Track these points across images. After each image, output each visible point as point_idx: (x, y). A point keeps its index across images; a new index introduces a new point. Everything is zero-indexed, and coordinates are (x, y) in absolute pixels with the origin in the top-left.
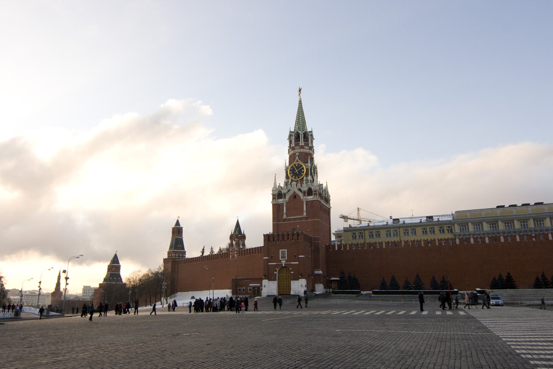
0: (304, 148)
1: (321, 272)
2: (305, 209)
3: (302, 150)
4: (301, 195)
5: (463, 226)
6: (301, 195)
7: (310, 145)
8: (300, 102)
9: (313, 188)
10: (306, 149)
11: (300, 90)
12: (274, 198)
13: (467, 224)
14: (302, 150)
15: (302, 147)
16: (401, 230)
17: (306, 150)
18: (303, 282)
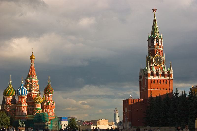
0: (151, 48)
3: (150, 49)
12: (140, 79)
14: (150, 49)
17: (152, 49)
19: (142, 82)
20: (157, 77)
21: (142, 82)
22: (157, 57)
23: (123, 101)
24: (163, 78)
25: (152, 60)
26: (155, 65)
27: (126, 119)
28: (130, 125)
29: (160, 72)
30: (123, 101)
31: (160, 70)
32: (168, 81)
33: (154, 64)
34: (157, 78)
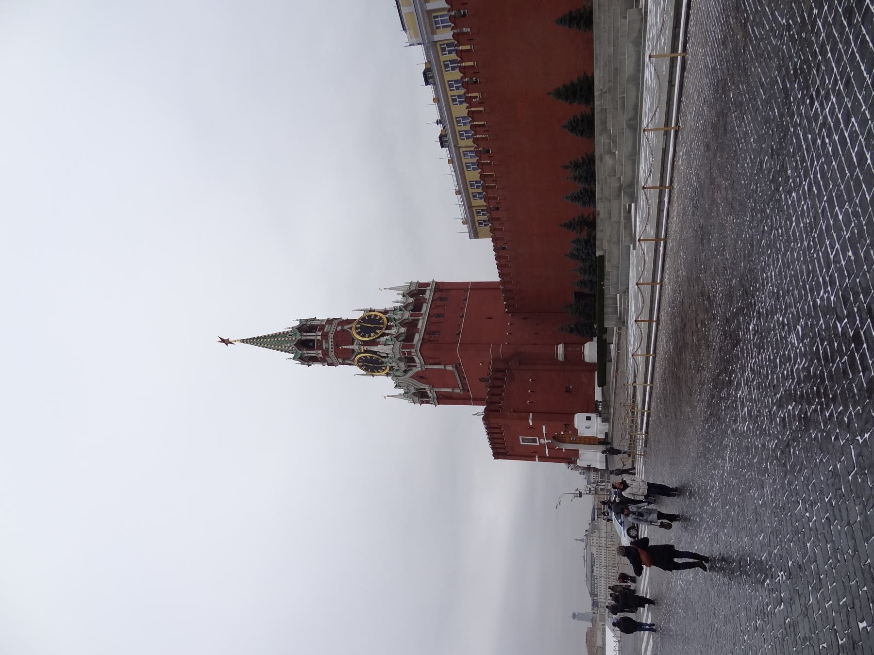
1: (560, 348)
2: (441, 367)
4: (415, 370)
5: (437, 23)
6: (415, 370)
7: (319, 338)
8: (243, 341)
9: (398, 356)
10: (327, 345)
11: (223, 341)
12: (428, 402)
13: (430, 12)
14: (332, 354)
15: (326, 353)
16: (462, 143)
17: (329, 345)
18: (579, 420)
19: (437, 390)
20: (421, 322)
21: (437, 390)
22: (357, 329)
23: (497, 455)
24: (425, 308)
25: (365, 343)
26: (383, 335)
27: (565, 447)
28: (589, 418)
29: (407, 315)
30: (497, 455)
31: (397, 317)
32: (438, 295)
33: (379, 337)
34: (422, 324)
